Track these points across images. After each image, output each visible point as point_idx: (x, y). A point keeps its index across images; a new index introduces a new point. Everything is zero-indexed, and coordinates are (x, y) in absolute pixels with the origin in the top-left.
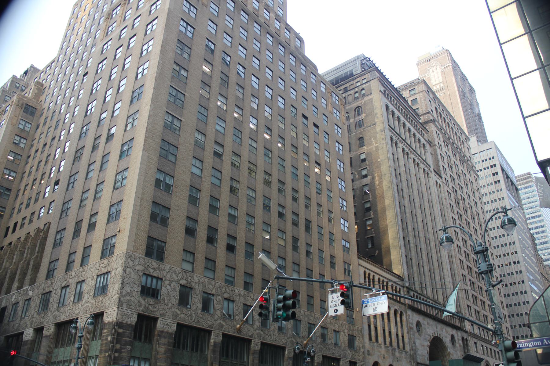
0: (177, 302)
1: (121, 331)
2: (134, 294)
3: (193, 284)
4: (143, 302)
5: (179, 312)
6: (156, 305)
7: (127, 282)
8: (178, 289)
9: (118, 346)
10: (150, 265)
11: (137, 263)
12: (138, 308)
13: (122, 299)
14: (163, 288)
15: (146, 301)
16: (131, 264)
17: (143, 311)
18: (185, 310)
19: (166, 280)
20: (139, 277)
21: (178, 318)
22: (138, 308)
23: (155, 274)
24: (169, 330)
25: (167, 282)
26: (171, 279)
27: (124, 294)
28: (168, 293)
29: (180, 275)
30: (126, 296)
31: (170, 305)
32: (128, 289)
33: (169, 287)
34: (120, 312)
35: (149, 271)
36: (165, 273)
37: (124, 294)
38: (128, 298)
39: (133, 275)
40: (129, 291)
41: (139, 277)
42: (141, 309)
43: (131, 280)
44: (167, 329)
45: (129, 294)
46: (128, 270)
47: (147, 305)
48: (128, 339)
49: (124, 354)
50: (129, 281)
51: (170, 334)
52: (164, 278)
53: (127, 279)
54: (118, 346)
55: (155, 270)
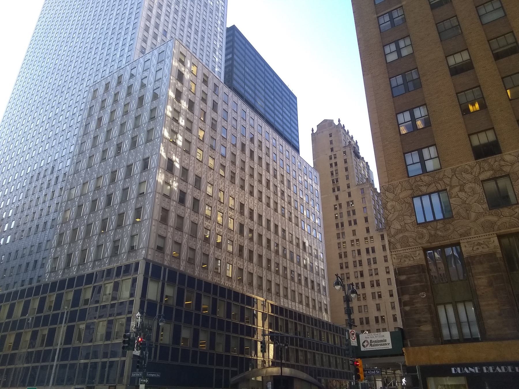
0: (486, 206)
1: (403, 278)
2: (408, 227)
3: (507, 169)
4: (425, 231)
5: (495, 219)
6: (448, 226)
7: (393, 218)
8: (479, 189)
9: (406, 298)
10: (420, 183)
11: (399, 191)
12: (419, 241)
13: (392, 240)
14: (452, 201)
15: (429, 227)
16: (391, 196)
17: (428, 242)
18: (506, 211)
19: (452, 187)
20: (407, 205)
21: (496, 227)
22: (419, 241)
23: (432, 188)
24: (486, 250)
25: (457, 189)
26: (461, 183)
27: (393, 233)
28: (464, 202)
29: (476, 170)
30: (397, 233)
31: (473, 215)
32: (396, 225)
33: (462, 195)
34: (394, 256)
35: (421, 191)
36: (447, 181)
37: (393, 233)
38: (401, 235)
39: (398, 207)
40: (399, 227)
41: (407, 205)
42: (424, 241)
43: (397, 214)
44: (480, 250)
45: (398, 232)
46: (389, 204)
47: (433, 232)
48: (418, 284)
49: (418, 305)
50: (395, 216)
51: (491, 256)
52: (448, 188)
53: (391, 215)
54: (406, 298)
55: (428, 185)
